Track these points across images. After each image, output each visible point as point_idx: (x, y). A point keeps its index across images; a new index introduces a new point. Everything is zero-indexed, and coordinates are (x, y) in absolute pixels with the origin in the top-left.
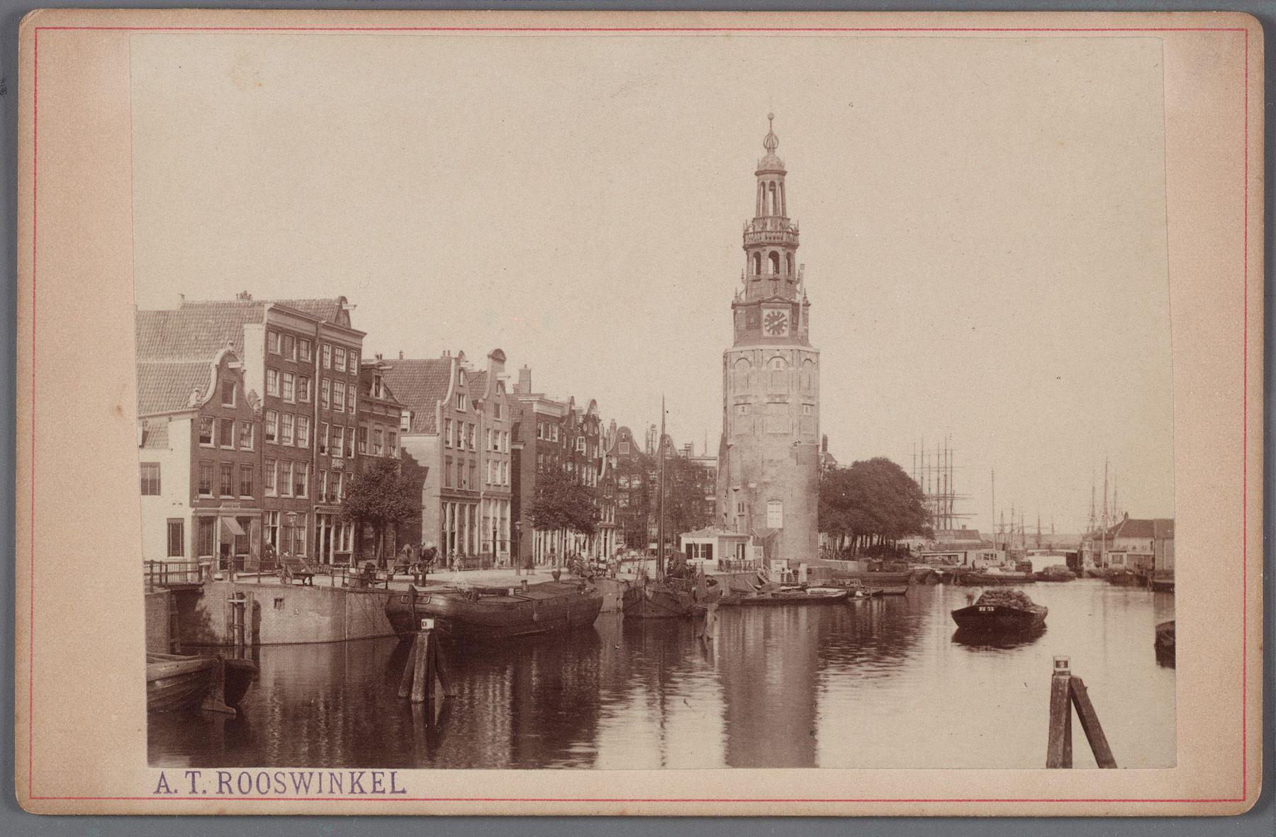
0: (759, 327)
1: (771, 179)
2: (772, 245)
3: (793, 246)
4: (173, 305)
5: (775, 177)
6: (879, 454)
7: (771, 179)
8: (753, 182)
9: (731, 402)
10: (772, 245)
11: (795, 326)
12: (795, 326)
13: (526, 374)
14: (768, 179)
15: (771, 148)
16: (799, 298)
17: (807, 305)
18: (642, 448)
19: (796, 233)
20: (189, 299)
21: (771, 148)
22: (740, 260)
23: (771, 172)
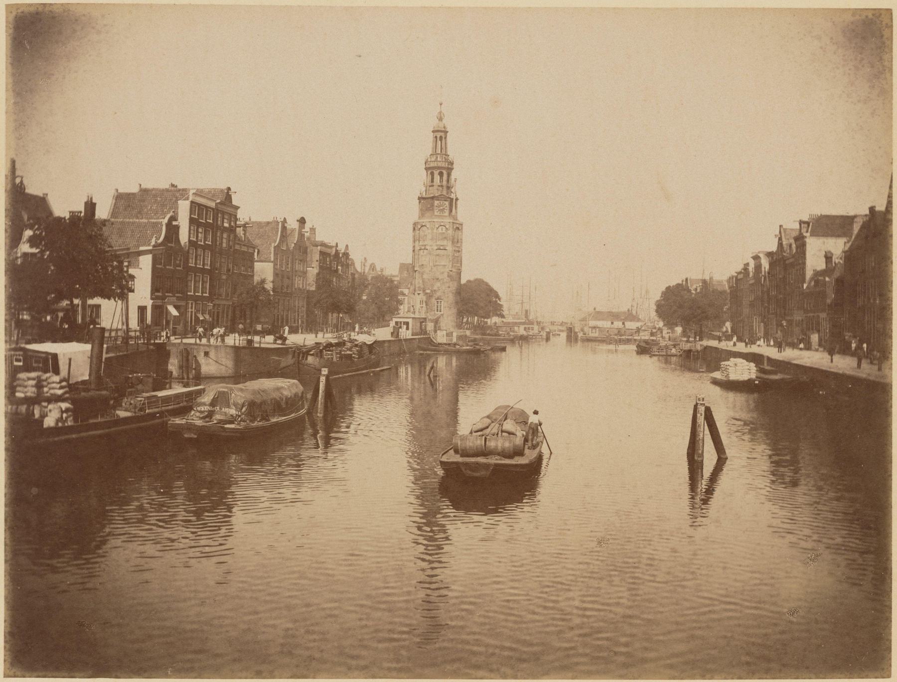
0: (433, 210)
1: (441, 135)
2: (441, 170)
3: (450, 170)
4: (135, 190)
5: (442, 134)
6: (479, 277)
7: (441, 135)
8: (431, 136)
9: (417, 248)
10: (441, 170)
11: (451, 211)
12: (451, 211)
13: (313, 230)
14: (438, 135)
15: (441, 119)
16: (453, 196)
17: (457, 199)
18: (359, 270)
19: (452, 164)
20: (143, 186)
21: (441, 119)
22: (423, 175)
23: (441, 131)
